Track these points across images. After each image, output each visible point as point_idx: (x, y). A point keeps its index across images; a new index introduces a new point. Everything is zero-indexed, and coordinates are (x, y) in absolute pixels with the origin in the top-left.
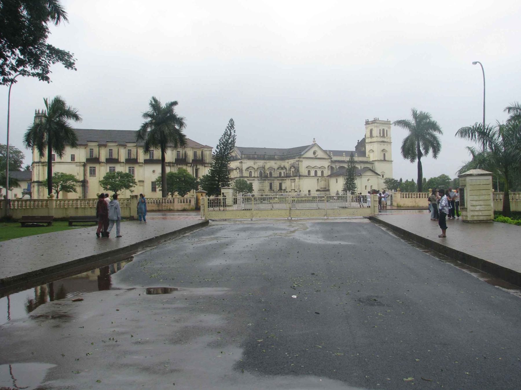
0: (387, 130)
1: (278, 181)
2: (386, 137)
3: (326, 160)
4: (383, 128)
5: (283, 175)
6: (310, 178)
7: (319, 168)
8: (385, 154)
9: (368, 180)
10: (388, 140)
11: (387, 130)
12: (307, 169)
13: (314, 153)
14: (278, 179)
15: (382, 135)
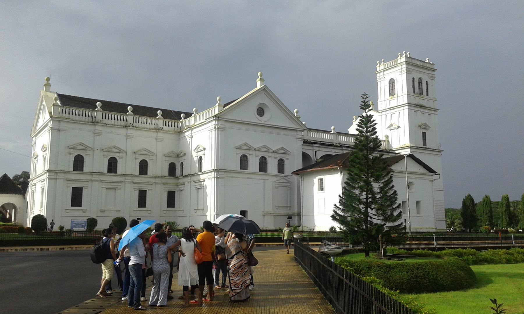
0: (427, 82)
1: (165, 186)
2: (426, 97)
3: (294, 133)
4: (420, 75)
5: (178, 172)
6: (244, 176)
7: (274, 152)
8: (425, 133)
9: (409, 188)
10: (431, 105)
11: (427, 82)
12: (238, 151)
13: (261, 112)
14: (164, 181)
15: (417, 90)
